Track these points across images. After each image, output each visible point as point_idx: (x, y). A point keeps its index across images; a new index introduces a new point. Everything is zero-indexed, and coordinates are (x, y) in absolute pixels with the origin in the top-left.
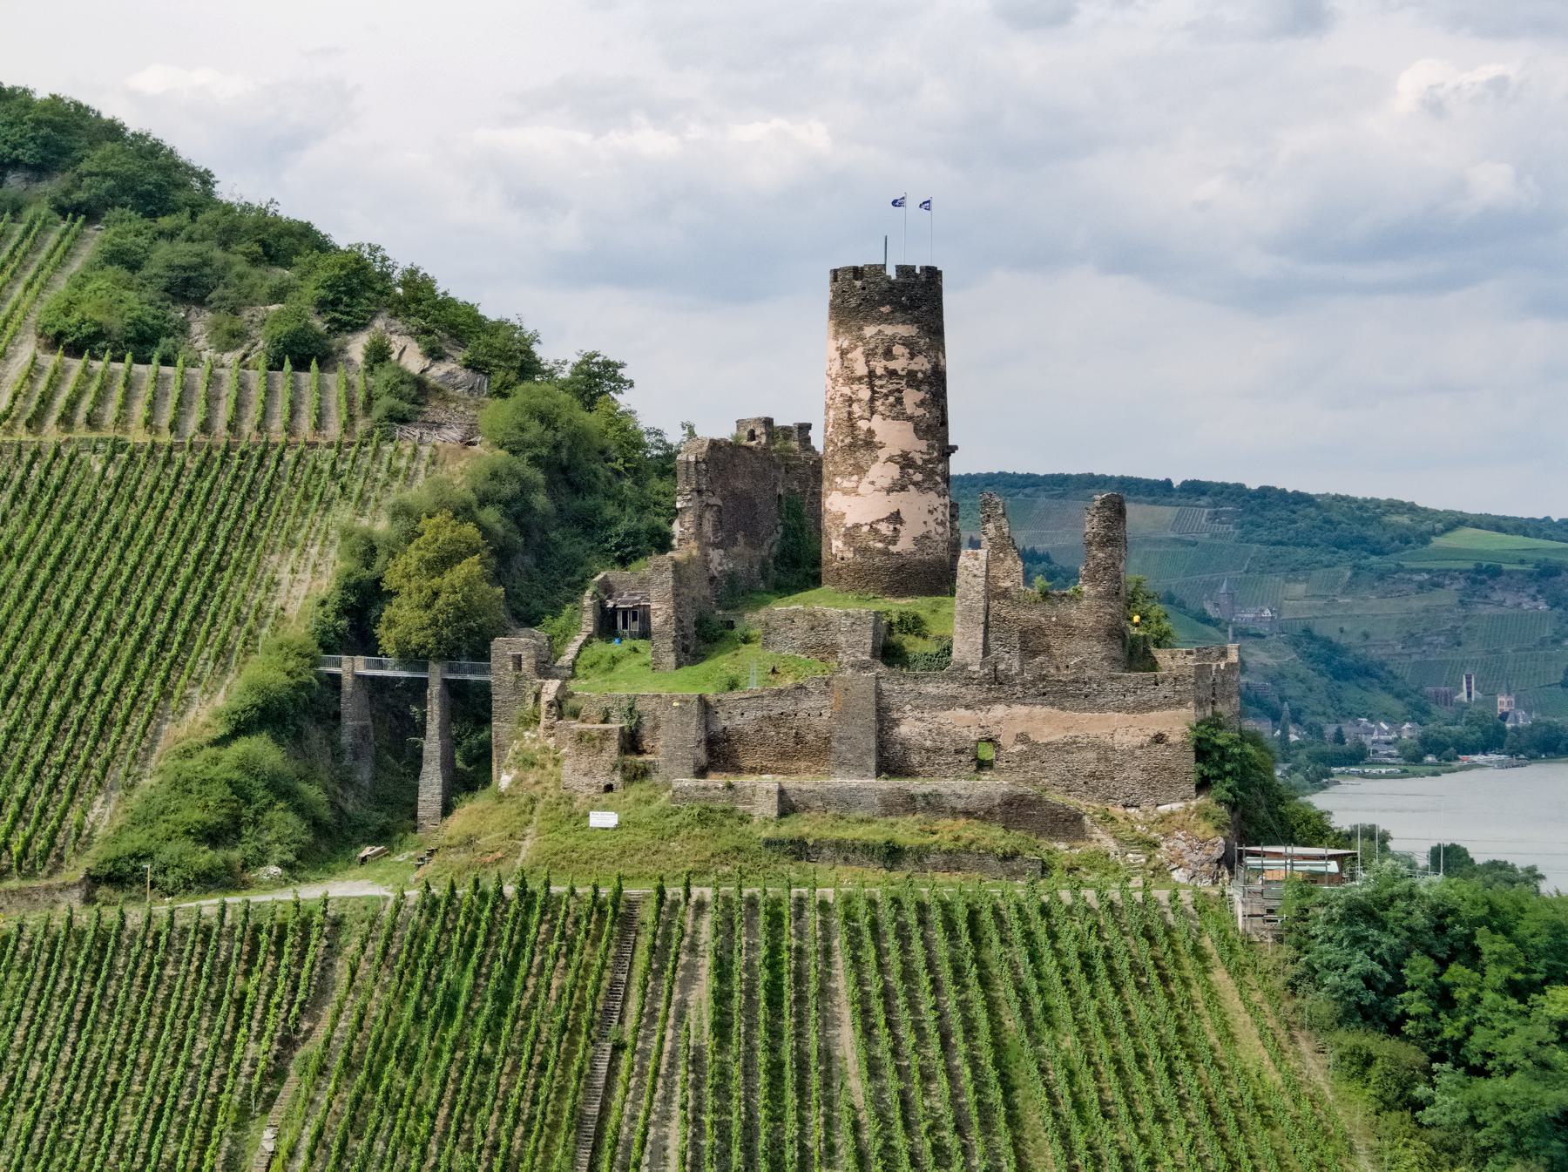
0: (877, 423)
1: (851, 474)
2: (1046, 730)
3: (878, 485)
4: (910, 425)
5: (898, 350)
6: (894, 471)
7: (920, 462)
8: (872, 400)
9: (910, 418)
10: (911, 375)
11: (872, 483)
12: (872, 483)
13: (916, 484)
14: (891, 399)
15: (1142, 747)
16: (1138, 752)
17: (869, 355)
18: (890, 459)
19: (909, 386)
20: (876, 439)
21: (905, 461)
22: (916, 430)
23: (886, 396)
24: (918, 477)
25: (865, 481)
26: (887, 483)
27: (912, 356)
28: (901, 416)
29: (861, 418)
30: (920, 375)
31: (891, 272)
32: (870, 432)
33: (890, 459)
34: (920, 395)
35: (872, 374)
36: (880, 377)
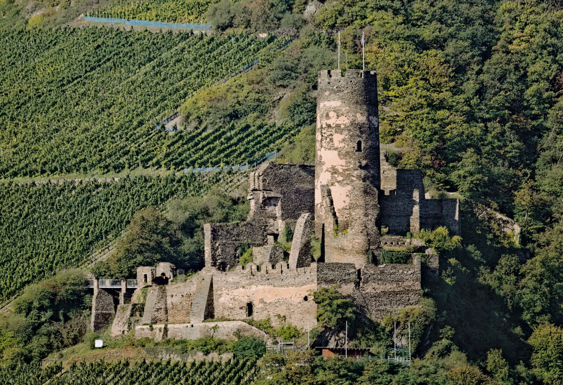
2: (269, 296)
4: (336, 152)
5: (332, 114)
7: (341, 171)
10: (338, 126)
13: (338, 182)
14: (328, 139)
19: (336, 132)
21: (334, 171)
22: (339, 155)
24: (340, 178)
30: (342, 126)
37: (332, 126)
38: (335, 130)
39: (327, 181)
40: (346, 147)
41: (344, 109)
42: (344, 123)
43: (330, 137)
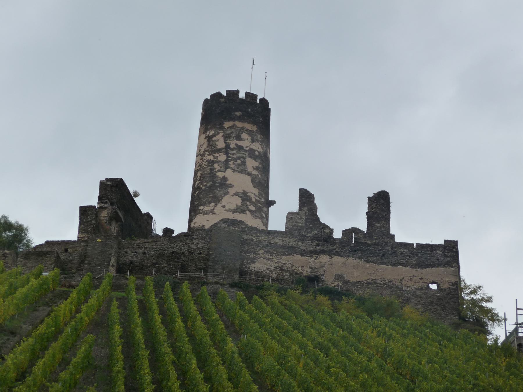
0: (229, 173)
1: (210, 202)
3: (227, 208)
5: (244, 136)
6: (238, 201)
7: (254, 200)
8: (227, 161)
9: (249, 174)
11: (224, 207)
12: (224, 207)
13: (251, 211)
15: (421, 289)
16: (419, 293)
17: (226, 137)
18: (236, 194)
19: (250, 157)
20: (228, 182)
22: (253, 181)
23: (236, 160)
24: (252, 208)
25: (219, 205)
26: (233, 207)
27: (253, 142)
28: (243, 171)
29: (219, 171)
31: (242, 95)
32: (225, 179)
33: (236, 194)
34: (256, 164)
35: (227, 147)
36: (233, 149)
37: (245, 148)
38: (249, 154)
39: (235, 206)
40: (260, 176)
41: (259, 136)
42: (259, 150)
43: (242, 159)
